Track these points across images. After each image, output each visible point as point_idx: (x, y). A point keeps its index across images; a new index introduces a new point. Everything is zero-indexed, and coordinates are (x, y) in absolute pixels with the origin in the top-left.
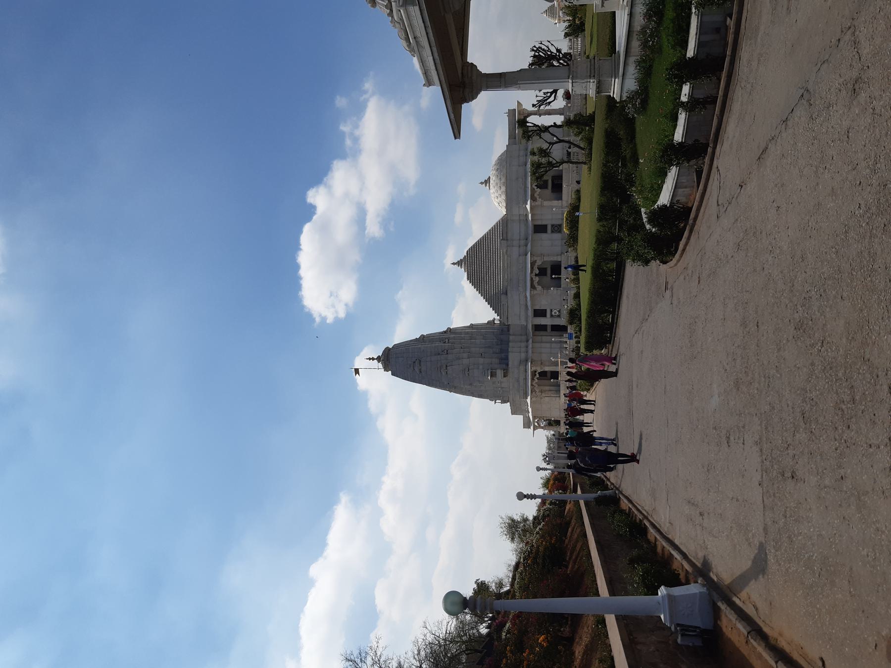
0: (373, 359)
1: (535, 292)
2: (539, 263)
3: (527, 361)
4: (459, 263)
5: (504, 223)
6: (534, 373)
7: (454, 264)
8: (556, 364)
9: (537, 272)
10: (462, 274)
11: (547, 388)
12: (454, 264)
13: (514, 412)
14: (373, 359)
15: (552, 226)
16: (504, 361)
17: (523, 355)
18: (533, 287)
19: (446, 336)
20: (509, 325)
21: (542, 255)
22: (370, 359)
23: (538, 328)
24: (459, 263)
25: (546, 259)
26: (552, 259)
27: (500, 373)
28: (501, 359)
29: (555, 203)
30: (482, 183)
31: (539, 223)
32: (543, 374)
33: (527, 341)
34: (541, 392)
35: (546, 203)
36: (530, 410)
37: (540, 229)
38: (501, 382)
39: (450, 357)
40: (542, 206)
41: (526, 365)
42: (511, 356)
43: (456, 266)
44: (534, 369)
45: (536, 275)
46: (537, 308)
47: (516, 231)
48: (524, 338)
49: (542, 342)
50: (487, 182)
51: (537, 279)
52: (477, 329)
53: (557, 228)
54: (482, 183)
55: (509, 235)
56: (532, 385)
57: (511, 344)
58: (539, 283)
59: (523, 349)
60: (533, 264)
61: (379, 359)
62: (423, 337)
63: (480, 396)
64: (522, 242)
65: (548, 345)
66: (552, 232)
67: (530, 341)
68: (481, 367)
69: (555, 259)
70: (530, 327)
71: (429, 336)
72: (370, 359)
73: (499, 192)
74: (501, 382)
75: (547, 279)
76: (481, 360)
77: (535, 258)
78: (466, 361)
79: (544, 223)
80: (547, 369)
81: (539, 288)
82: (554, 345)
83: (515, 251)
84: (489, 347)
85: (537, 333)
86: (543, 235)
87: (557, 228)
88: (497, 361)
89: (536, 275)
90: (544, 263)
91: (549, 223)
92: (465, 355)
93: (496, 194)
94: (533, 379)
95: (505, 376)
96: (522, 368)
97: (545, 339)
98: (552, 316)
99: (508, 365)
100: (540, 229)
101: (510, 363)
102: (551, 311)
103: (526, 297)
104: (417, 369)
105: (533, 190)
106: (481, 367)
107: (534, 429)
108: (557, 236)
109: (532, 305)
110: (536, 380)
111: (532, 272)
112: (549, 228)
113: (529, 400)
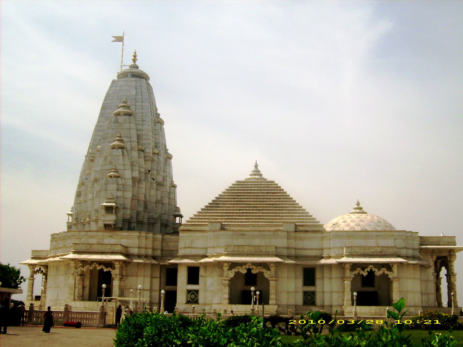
0: (134, 60)
1: (226, 268)
2: (267, 274)
3: (126, 255)
4: (257, 172)
5: (317, 230)
6: (109, 264)
7: (256, 166)
8: (122, 294)
9: (254, 272)
10: (244, 174)
11: (87, 283)
12: (256, 166)
13: (55, 238)
14: (134, 60)
15: (313, 293)
16: (127, 225)
17: (135, 251)
18: (233, 265)
19: (162, 152)
21: (276, 277)
22: (135, 56)
23: (171, 275)
24: (257, 172)
25: (272, 283)
26: (272, 291)
27: (111, 218)
28: (130, 223)
29: (348, 296)
30: (358, 204)
31: (318, 275)
32: (106, 278)
33: (154, 258)
34: (82, 275)
35: (348, 283)
36: (57, 259)
37: (309, 276)
38: (96, 221)
39: (135, 154)
40: (343, 278)
41: (121, 254)
42: (136, 234)
43: (253, 169)
44: (117, 265)
45: (249, 270)
46: (201, 272)
47: (309, 245)
48: (158, 253)
49: (152, 277)
50: (359, 209)
52: (169, 193)
53: (309, 299)
54: (358, 204)
55: (302, 235)
56: (92, 262)
57: (151, 235)
58: (237, 274)
59: (143, 252)
60: (265, 265)
62: (161, 123)
63: (79, 195)
64: (293, 252)
65: (148, 286)
66: (305, 293)
68: (120, 194)
69: (272, 296)
71: (162, 130)
72: (135, 56)
73: (352, 224)
74: (96, 221)
75: (241, 286)
76: (129, 195)
77: (273, 269)
78: (128, 174)
79: (318, 282)
80: (116, 283)
81: (231, 274)
82: (147, 294)
83: (282, 242)
84: (146, 207)
85: (164, 272)
86: (300, 281)
87: (309, 299)
88: (128, 217)
89: (249, 270)
90: (268, 281)
91: (318, 288)
92: (136, 174)
93: (349, 220)
94: (100, 263)
95: (107, 226)
96: (119, 248)
97: (156, 282)
98: (189, 291)
99: (121, 229)
100: (309, 276)
101: (125, 233)
102: (197, 291)
103: (218, 256)
104: (121, 110)
105: (363, 266)
106: (120, 194)
107: (30, 265)
108: (300, 300)
109: (206, 265)
110: (99, 268)
111: (254, 264)
112: (311, 289)
113: (71, 256)
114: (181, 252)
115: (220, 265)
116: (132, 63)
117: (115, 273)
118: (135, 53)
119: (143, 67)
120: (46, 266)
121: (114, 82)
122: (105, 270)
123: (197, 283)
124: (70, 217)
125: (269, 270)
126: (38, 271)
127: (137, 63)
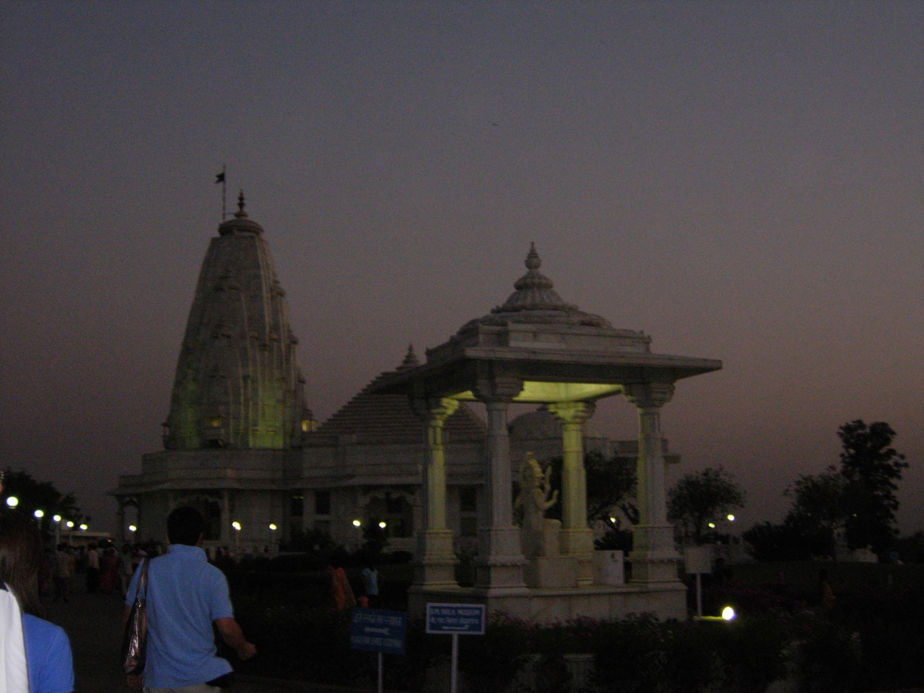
0: (241, 205)
2: (410, 499)
7: (411, 349)
9: (395, 495)
12: (411, 349)
14: (241, 205)
18: (367, 489)
20: (300, 448)
22: (241, 199)
43: (406, 353)
45: (388, 494)
51: (381, 495)
61: (239, 215)
67: (274, 487)
70: (298, 485)
72: (241, 199)
114: (306, 474)
115: (352, 488)
116: (237, 209)
117: (225, 503)
118: (241, 194)
119: (253, 214)
120: (138, 496)
121: (214, 241)
122: (211, 500)
123: (327, 513)
124: (167, 429)
125: (413, 494)
126: (128, 503)
127: (245, 210)
